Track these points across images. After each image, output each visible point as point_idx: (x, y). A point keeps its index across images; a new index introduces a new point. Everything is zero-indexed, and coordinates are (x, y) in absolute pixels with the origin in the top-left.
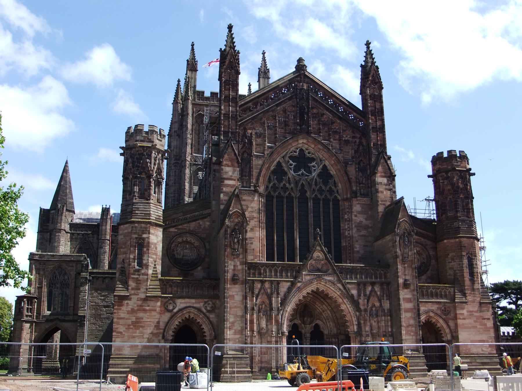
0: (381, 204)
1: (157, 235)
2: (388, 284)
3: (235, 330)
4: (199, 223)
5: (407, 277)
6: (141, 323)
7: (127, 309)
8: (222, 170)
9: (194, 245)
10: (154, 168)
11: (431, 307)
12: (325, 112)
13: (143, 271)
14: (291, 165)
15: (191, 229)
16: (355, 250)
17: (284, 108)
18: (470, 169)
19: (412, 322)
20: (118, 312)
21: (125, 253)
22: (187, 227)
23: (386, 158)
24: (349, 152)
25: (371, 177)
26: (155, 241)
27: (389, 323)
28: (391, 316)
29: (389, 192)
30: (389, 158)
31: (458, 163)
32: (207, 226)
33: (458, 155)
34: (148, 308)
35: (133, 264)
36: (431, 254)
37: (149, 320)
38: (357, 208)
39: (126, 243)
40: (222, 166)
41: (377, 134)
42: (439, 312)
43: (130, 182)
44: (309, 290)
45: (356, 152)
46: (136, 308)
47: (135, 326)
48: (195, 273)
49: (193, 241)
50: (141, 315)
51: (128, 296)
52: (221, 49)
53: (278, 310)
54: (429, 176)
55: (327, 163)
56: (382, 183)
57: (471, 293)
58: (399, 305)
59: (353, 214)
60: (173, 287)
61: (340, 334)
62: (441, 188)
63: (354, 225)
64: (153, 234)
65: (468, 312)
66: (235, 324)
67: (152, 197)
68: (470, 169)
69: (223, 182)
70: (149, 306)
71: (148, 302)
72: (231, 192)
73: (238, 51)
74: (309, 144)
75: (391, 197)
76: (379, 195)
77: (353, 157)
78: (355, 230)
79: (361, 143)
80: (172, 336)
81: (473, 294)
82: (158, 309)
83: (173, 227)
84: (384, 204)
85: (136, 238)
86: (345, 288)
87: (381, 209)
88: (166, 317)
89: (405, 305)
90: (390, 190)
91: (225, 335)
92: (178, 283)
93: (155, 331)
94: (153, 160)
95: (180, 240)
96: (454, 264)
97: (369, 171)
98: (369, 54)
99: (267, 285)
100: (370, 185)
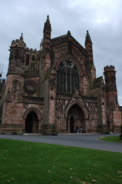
5: (103, 101)
6: (15, 112)
8: (45, 60)
14: (65, 63)
19: (104, 115)
24: (82, 62)
27: (97, 116)
29: (95, 75)
38: (85, 79)
39: (10, 81)
44: (73, 103)
45: (85, 62)
46: (13, 106)
47: (13, 113)
50: (15, 109)
53: (65, 110)
58: (102, 110)
61: (80, 119)
70: (18, 106)
77: (83, 63)
79: (86, 60)
80: (26, 117)
82: (22, 107)
83: (27, 78)
86: (85, 103)
87: (93, 80)
88: (25, 110)
89: (103, 110)
96: (112, 99)
98: (88, 34)
99: (61, 101)
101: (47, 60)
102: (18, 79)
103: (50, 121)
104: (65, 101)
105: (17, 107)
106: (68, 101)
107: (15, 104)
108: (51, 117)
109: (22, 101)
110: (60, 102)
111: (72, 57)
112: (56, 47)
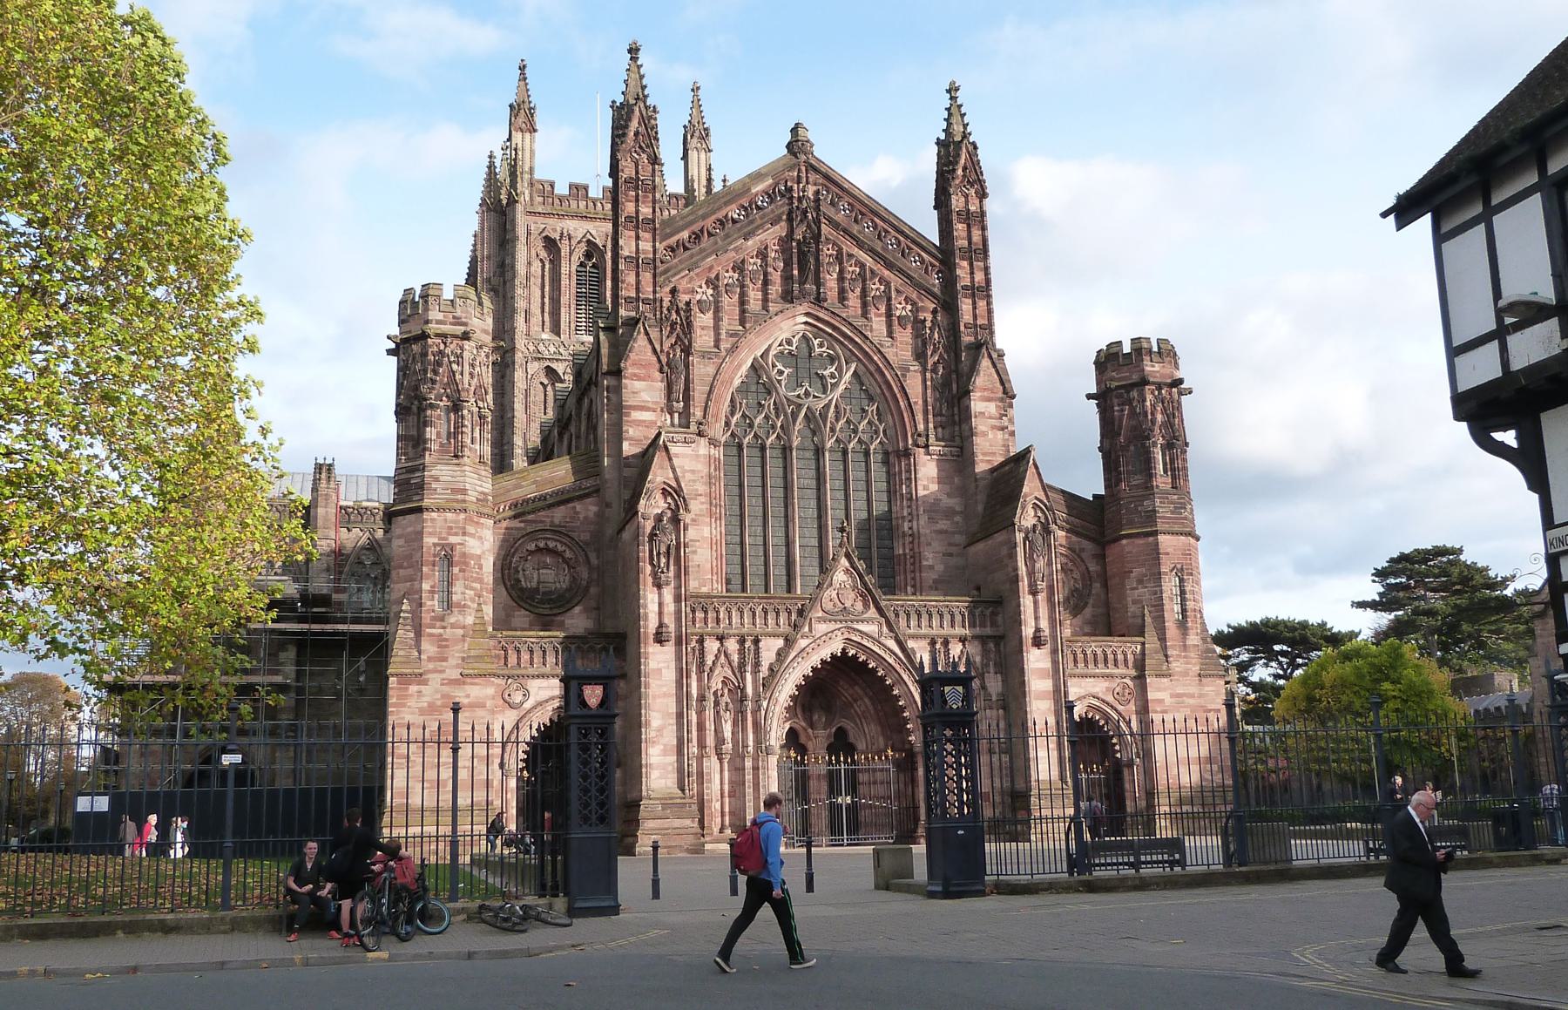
0: (982, 461)
1: (480, 538)
2: (999, 639)
3: (665, 745)
4: (575, 507)
7: (420, 705)
9: (563, 557)
10: (470, 385)
11: (1094, 686)
13: (452, 620)
14: (781, 373)
15: (557, 521)
16: (925, 563)
17: (761, 242)
18: (1181, 381)
20: (398, 712)
21: (411, 579)
22: (548, 517)
23: (995, 356)
25: (959, 399)
26: (478, 552)
28: (1004, 708)
29: (1000, 434)
30: (1001, 355)
31: (1153, 366)
32: (591, 515)
33: (1155, 349)
35: (429, 603)
36: (1091, 569)
40: (626, 378)
42: (1110, 699)
43: (415, 417)
44: (825, 654)
48: (566, 622)
49: (560, 548)
52: (614, 102)
54: (1089, 397)
56: (984, 413)
57: (1179, 656)
63: (922, 509)
64: (472, 535)
65: (1172, 696)
66: (665, 732)
67: (467, 452)
68: (1181, 381)
69: (628, 415)
72: (646, 438)
73: (654, 107)
75: (1004, 446)
78: (923, 520)
81: (1185, 657)
85: (435, 545)
90: (1003, 429)
91: (643, 756)
92: (533, 643)
94: (466, 367)
95: (532, 547)
97: (954, 386)
98: (954, 111)
99: (732, 645)
100: (957, 418)
101: (638, 385)
102: (453, 539)
103: (654, 774)
104: (756, 641)
107: (446, 689)
108: (665, 753)
110: (726, 655)
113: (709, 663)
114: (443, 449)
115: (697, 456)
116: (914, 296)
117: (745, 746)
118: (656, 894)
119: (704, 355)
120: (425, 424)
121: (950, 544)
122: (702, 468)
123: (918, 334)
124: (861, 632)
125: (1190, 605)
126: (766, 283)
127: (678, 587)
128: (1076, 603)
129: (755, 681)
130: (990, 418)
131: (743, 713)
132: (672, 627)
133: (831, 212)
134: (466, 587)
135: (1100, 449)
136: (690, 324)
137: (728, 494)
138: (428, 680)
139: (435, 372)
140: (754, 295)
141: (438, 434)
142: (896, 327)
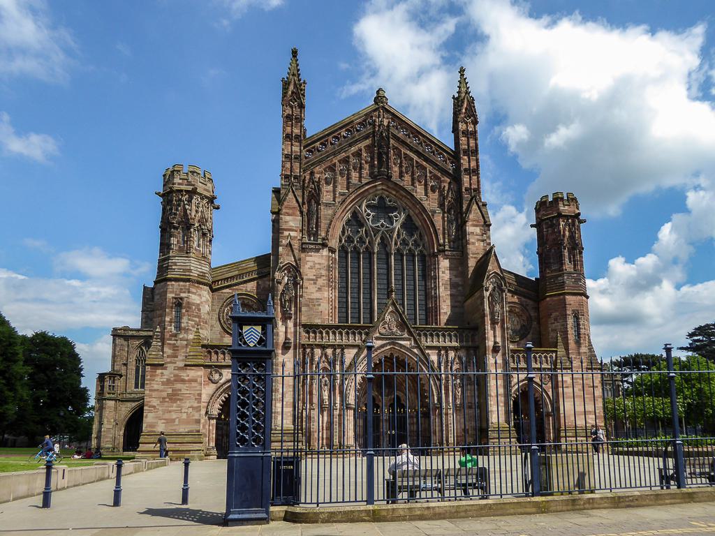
0: (472, 257)
2: (476, 348)
7: (162, 380)
12: (408, 152)
13: (181, 336)
14: (369, 215)
15: (249, 290)
23: (480, 204)
25: (462, 227)
26: (198, 302)
29: (482, 244)
30: (485, 205)
33: (566, 198)
34: (187, 378)
35: (169, 327)
37: (188, 392)
40: (281, 214)
41: (470, 177)
46: (172, 379)
47: (170, 399)
50: (178, 386)
51: (163, 365)
54: (532, 226)
55: (412, 213)
59: (440, 270)
60: (219, 354)
62: (545, 238)
69: (283, 233)
70: (188, 376)
71: (188, 371)
74: (390, 190)
76: (470, 247)
84: (475, 258)
90: (483, 241)
93: (196, 405)
100: (460, 237)
101: (288, 218)
102: (183, 295)
105: (183, 381)
106: (355, 351)
107: (177, 372)
109: (201, 362)
111: (394, 190)
112: (329, 164)
113: (317, 359)
114: (181, 249)
115: (322, 256)
116: (439, 175)
117: (335, 404)
118: (117, 503)
119: (327, 205)
120: (171, 236)
121: (456, 302)
122: (324, 262)
123: (441, 194)
124: (401, 344)
125: (582, 331)
126: (361, 168)
127: (296, 319)
128: (521, 334)
129: (342, 369)
130: (477, 235)
131: (334, 386)
132: (292, 340)
133: (396, 132)
134: (189, 320)
135: (537, 253)
136: (320, 190)
137: (340, 277)
138: (167, 367)
139: (177, 210)
140: (355, 175)
141: (178, 241)
142: (429, 190)
